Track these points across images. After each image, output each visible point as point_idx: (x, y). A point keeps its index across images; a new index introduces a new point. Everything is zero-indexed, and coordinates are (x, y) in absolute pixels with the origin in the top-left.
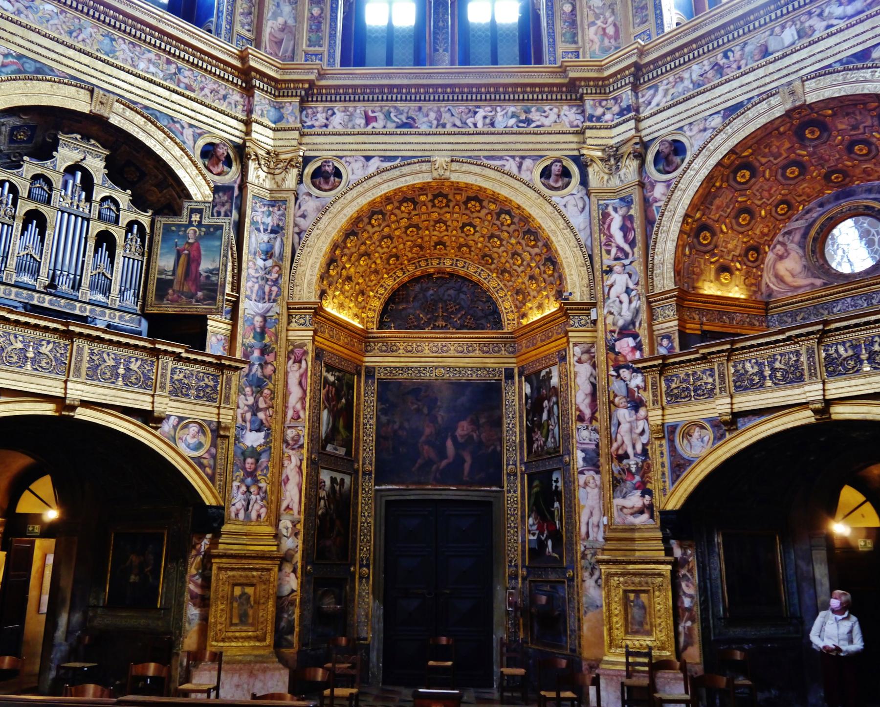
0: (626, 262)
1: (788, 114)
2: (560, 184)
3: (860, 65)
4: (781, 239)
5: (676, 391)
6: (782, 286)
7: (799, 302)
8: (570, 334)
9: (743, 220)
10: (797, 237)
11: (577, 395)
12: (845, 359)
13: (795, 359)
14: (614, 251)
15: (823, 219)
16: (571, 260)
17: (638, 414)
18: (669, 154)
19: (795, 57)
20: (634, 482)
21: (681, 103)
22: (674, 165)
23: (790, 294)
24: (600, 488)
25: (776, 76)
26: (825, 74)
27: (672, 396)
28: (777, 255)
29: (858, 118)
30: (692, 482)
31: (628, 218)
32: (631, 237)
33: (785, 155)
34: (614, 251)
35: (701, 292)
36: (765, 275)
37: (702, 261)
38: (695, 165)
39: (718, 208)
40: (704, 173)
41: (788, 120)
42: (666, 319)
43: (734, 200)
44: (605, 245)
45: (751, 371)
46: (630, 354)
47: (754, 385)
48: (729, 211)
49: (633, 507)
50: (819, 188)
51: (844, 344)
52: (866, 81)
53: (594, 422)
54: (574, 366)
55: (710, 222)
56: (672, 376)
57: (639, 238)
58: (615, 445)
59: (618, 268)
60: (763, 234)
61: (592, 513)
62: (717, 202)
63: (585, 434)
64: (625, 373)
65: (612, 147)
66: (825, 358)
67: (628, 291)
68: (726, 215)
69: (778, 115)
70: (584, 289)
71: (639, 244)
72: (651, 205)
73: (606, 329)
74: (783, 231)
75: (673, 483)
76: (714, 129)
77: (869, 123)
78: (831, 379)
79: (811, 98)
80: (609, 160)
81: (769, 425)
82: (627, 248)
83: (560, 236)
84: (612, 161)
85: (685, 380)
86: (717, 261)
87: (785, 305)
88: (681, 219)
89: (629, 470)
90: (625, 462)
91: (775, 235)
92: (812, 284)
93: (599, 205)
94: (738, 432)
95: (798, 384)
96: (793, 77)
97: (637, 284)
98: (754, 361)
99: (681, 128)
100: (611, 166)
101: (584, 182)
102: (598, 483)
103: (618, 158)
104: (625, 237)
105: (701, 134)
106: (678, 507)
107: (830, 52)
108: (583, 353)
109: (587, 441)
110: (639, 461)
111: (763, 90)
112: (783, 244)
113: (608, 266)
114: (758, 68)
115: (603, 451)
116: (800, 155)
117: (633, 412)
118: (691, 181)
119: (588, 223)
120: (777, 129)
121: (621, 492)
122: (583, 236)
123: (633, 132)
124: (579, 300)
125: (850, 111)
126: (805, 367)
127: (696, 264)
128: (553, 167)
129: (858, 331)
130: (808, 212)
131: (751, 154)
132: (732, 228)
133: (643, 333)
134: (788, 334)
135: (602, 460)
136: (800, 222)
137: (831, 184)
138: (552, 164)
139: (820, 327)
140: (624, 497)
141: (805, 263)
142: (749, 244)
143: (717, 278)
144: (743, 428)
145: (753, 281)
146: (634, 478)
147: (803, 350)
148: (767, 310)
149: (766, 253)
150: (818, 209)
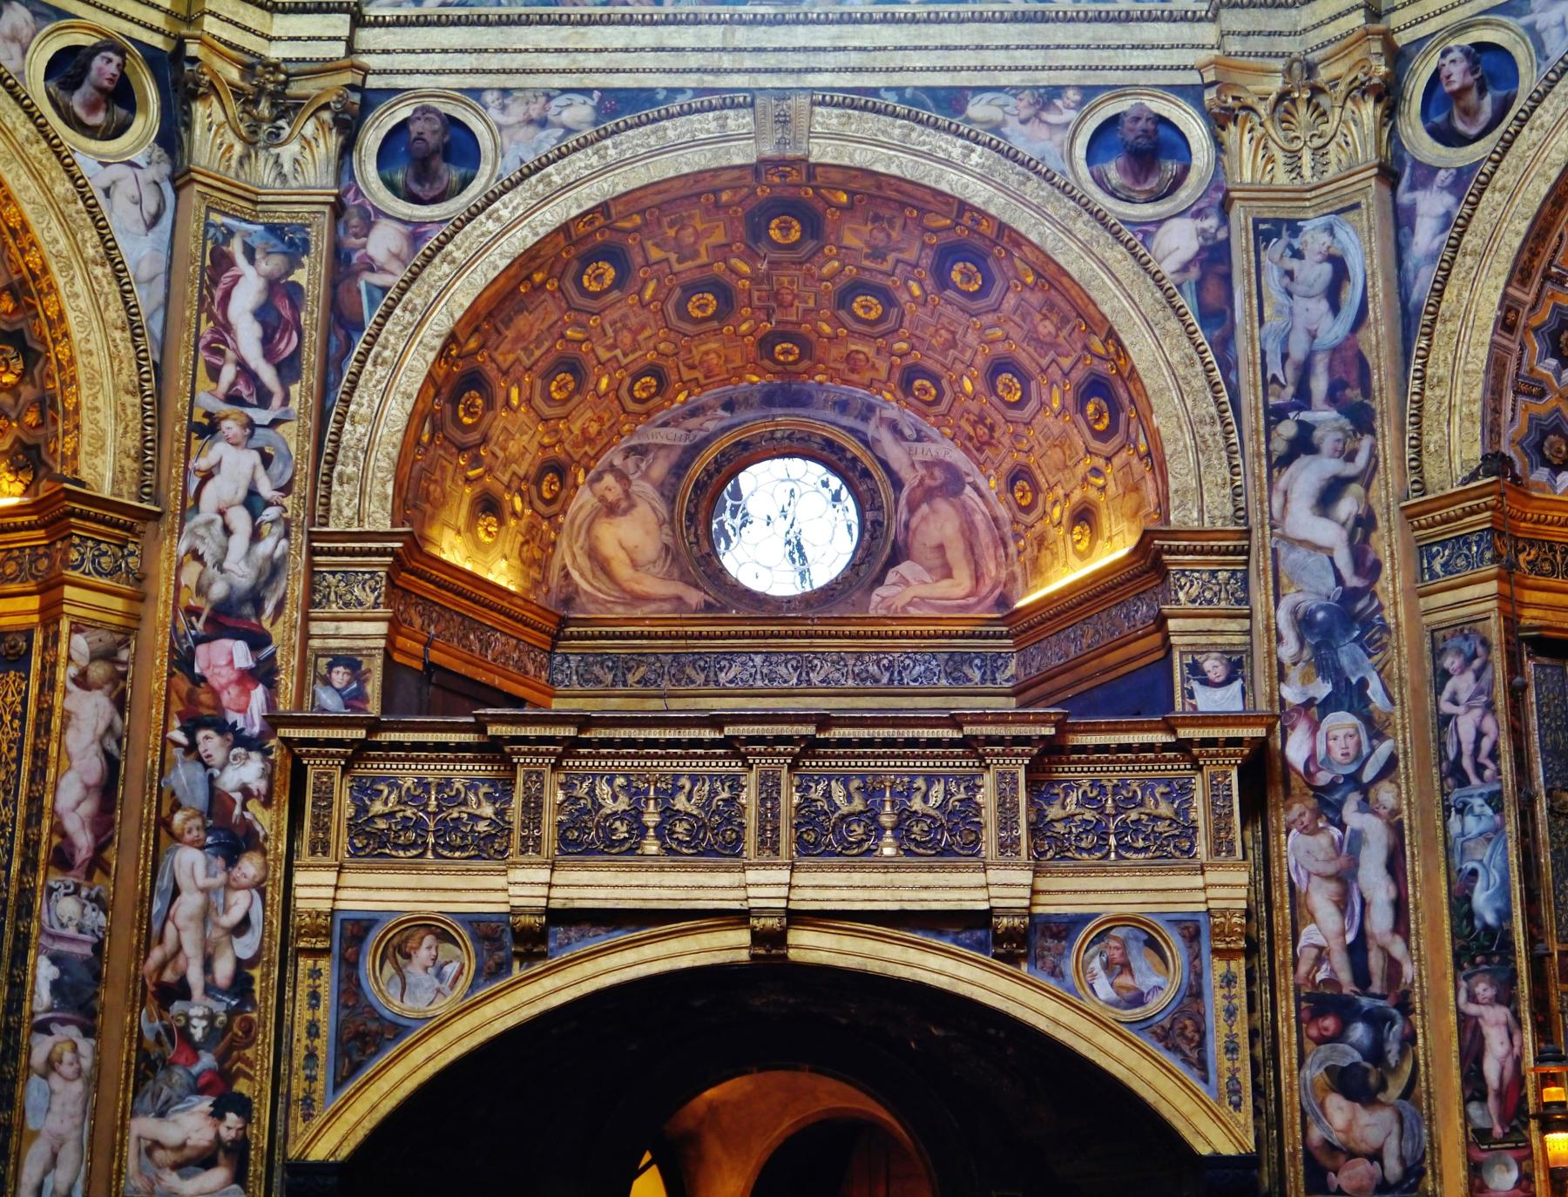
0: (261, 416)
1: (760, 168)
2: (99, 119)
3: (944, 121)
4: (618, 462)
5: (382, 824)
6: (604, 585)
7: (642, 636)
8: (69, 592)
9: (559, 388)
10: (660, 469)
11: (63, 784)
12: (843, 818)
13: (725, 795)
14: (228, 373)
15: (725, 442)
16: (101, 361)
17: (236, 873)
18: (435, 152)
19: (801, 35)
20: (196, 1069)
21: (488, 24)
22: (439, 187)
23: (620, 611)
24: (88, 1082)
25: (749, 61)
26: (864, 108)
27: (369, 835)
28: (602, 499)
29: (894, 234)
30: (396, 1087)
31: (280, 291)
32: (286, 347)
33: (704, 259)
34: (228, 373)
35: (435, 551)
36: (563, 544)
37: (450, 468)
38: (506, 208)
39: (520, 338)
40: (520, 240)
41: (750, 180)
42: (355, 611)
43: (556, 330)
44: (208, 347)
45: (610, 806)
46: (234, 691)
47: (613, 844)
48: (538, 353)
49: (183, 1146)
50: (738, 363)
51: (845, 780)
52: (948, 162)
53: (98, 873)
54: (66, 692)
55: (491, 370)
56: (375, 780)
57: (311, 357)
58: (157, 954)
59: (231, 427)
60: (587, 439)
61: (54, 1157)
62: (522, 322)
63: (68, 907)
64: (210, 743)
65: (276, 67)
66: (798, 808)
67: (253, 501)
68: (528, 363)
69: (738, 161)
70: (128, 463)
71: (310, 376)
72: (356, 275)
73: (176, 599)
74: (625, 443)
75: (338, 1085)
76: (569, 131)
77: (911, 255)
78: (806, 861)
79: (822, 152)
80: (256, 103)
81: (630, 956)
82: (268, 375)
83: (79, 283)
84: (264, 108)
85: (414, 798)
86: (479, 478)
87: (607, 636)
88: (438, 343)
89: (185, 1032)
90: (177, 1007)
91: (609, 444)
92: (679, 598)
93: (208, 225)
94: (550, 963)
95: (727, 861)
96: (790, 82)
97: (286, 489)
98: (620, 781)
99: (476, 93)
100: (258, 121)
101: (172, 138)
102: (86, 1063)
103: (288, 108)
104: (268, 343)
105: (531, 129)
106: (344, 1153)
107: (880, 60)
108: (95, 657)
109: (71, 931)
110: (219, 1008)
111: (710, 81)
112: (622, 477)
113: (208, 415)
114: (709, 22)
115: (118, 965)
116: (733, 270)
117: (220, 862)
118: (485, 248)
119: (162, 268)
120: (716, 192)
121: (155, 1096)
122: (147, 299)
123: (339, 49)
124: (106, 493)
125: (886, 213)
126: (751, 820)
127: (437, 476)
128: (98, 62)
129: (884, 756)
130: (694, 413)
131: (636, 230)
132: (529, 401)
133: (280, 633)
134: (729, 731)
135: (111, 997)
136: (671, 431)
137: (767, 363)
138: (95, 50)
139: (810, 730)
140: (161, 1114)
141: (669, 540)
142: (550, 453)
143: (471, 526)
144: (566, 955)
145: (537, 554)
146: (197, 1059)
147: (751, 780)
148: (556, 638)
149: (576, 487)
150: (721, 413)
